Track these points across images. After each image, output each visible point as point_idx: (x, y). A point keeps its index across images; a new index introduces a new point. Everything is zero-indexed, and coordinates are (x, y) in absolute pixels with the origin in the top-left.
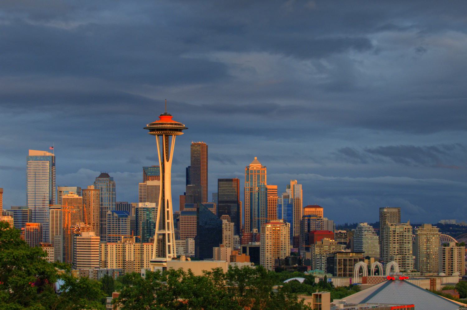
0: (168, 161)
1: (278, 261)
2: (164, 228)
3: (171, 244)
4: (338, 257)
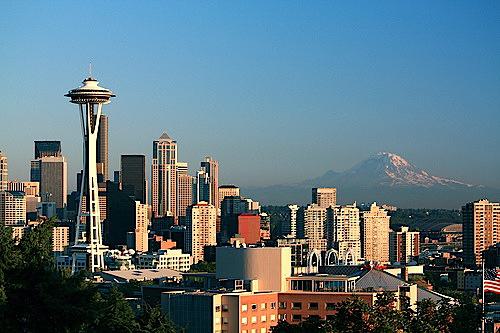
0: (93, 132)
1: (206, 248)
2: (88, 209)
3: (96, 228)
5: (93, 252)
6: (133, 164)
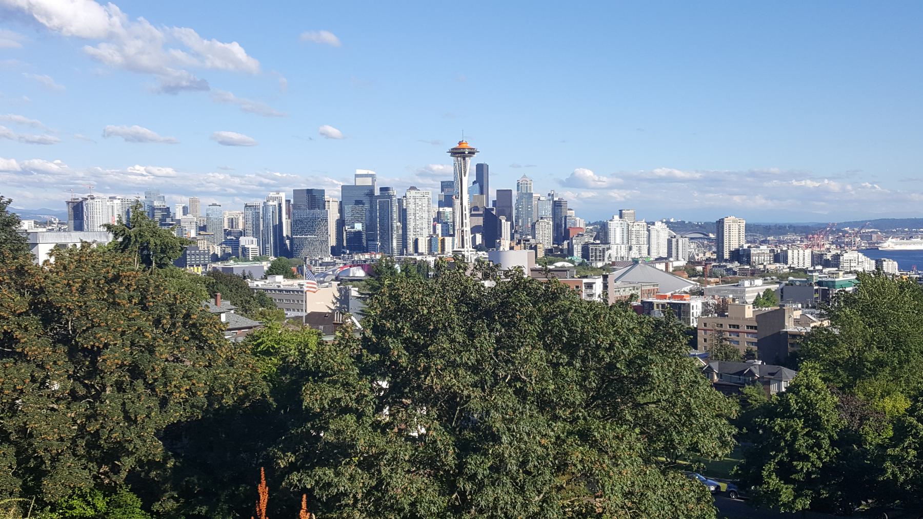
4: (591, 247)
5: (466, 254)
6: (504, 195)
